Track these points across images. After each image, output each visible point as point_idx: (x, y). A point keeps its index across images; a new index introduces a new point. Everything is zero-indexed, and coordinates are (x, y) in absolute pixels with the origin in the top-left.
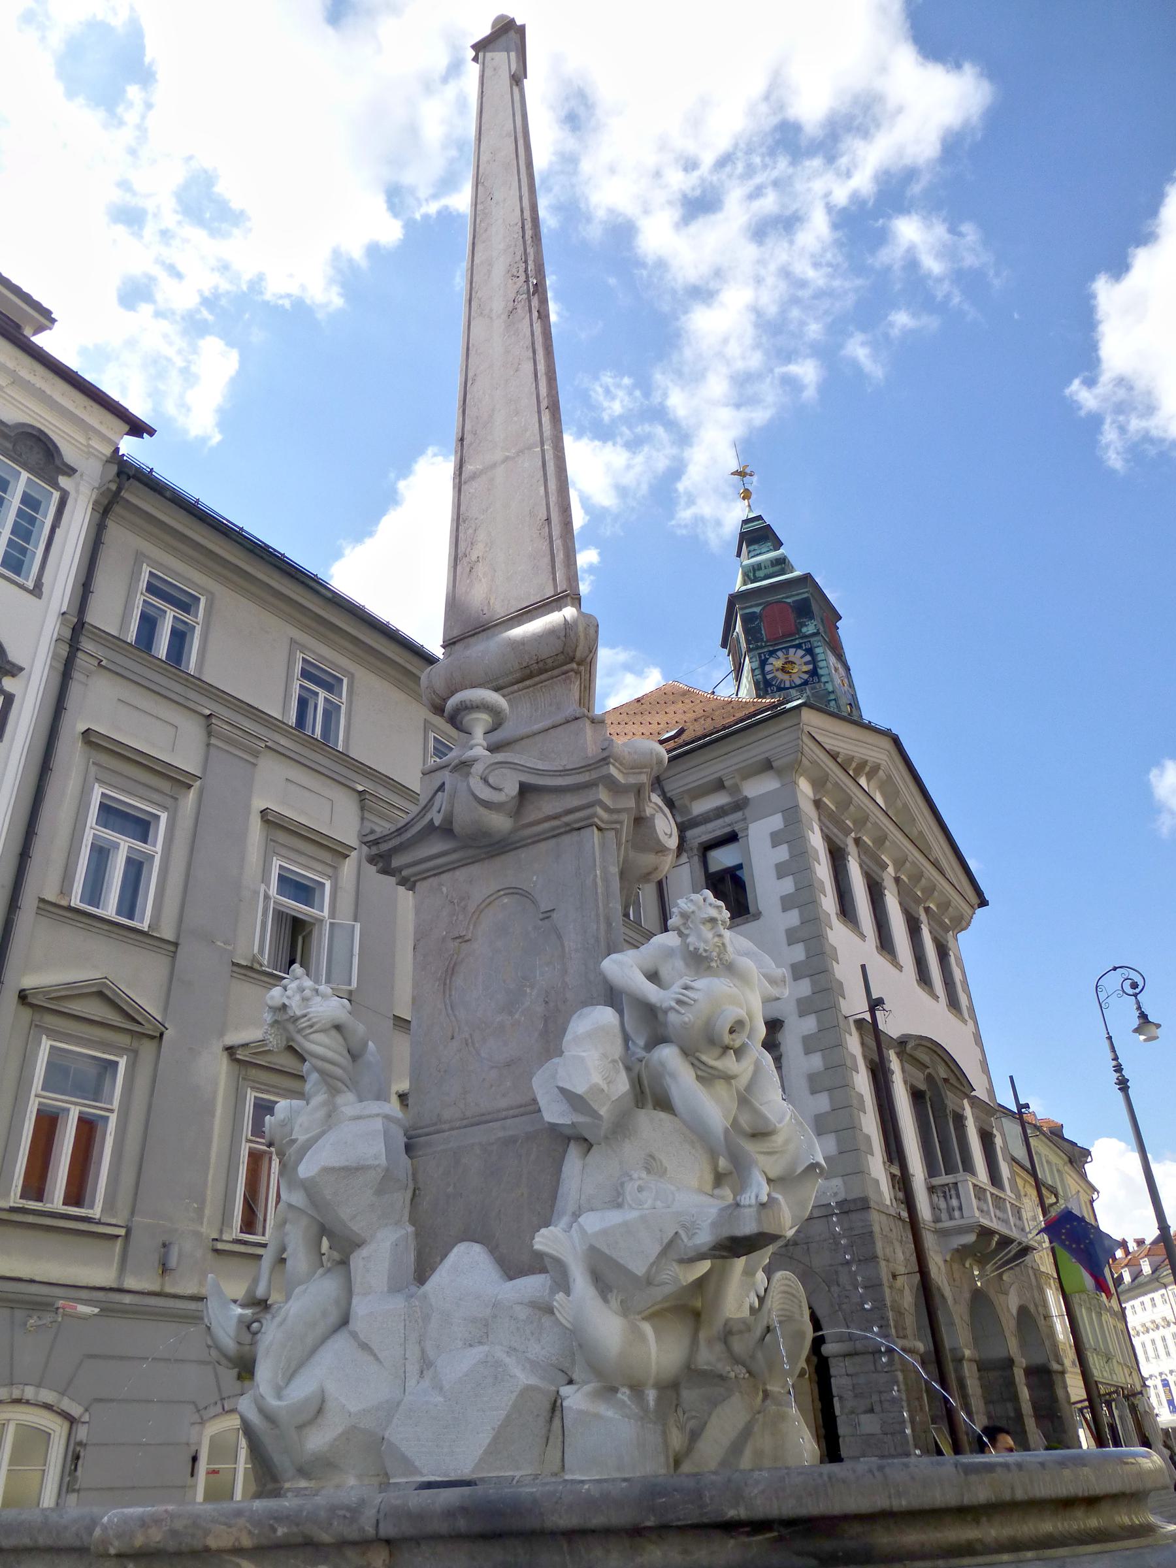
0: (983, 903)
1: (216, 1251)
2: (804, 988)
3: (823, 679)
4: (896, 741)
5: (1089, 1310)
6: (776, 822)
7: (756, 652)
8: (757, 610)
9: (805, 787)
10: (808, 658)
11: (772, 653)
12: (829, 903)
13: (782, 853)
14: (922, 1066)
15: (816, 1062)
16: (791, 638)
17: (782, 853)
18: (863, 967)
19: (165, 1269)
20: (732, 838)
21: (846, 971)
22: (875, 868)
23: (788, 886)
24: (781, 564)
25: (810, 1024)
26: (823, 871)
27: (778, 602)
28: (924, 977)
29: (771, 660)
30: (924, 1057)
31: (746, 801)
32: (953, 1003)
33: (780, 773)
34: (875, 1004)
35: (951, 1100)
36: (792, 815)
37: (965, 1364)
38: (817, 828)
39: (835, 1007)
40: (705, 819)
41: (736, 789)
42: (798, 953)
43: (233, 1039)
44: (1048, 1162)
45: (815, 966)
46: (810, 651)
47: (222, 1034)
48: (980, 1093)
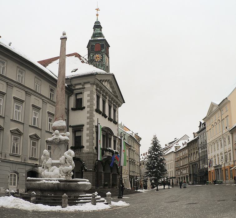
1: (10, 155)
2: (88, 120)
3: (103, 62)
4: (113, 76)
5: (132, 165)
6: (89, 93)
7: (92, 53)
8: (94, 44)
9: (95, 87)
10: (101, 57)
11: (95, 54)
13: (89, 98)
14: (105, 132)
15: (88, 132)
16: (99, 52)
17: (89, 98)
18: (98, 118)
19: (5, 157)
20: (81, 93)
21: (95, 119)
22: (105, 99)
24: (101, 35)
25: (88, 126)
26: (95, 102)
27: (98, 43)
29: (95, 55)
33: (91, 84)
34: (98, 124)
37: (102, 173)
38: (95, 94)
42: (88, 115)
43: (11, 129)
44: (132, 141)
45: (91, 118)
46: (102, 55)
47: (9, 129)
48: (115, 135)
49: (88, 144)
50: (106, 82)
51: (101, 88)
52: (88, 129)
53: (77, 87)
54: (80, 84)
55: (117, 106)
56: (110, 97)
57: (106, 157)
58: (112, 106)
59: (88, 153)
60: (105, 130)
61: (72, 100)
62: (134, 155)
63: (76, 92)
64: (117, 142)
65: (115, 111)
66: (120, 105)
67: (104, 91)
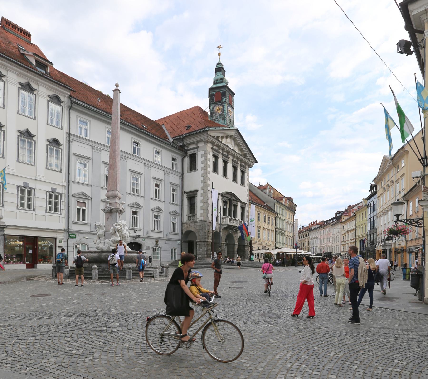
0: (256, 162)
2: (202, 185)
9: (210, 145)
12: (211, 168)
21: (210, 183)
23: (202, 166)
25: (202, 191)
26: (211, 163)
28: (235, 179)
30: (229, 196)
31: (198, 147)
32: (242, 183)
33: (204, 142)
35: (234, 203)
36: (205, 151)
39: (207, 189)
40: (191, 149)
41: (196, 144)
42: (202, 179)
45: (205, 182)
49: (202, 211)
50: (228, 139)
51: (219, 146)
52: (202, 195)
53: (191, 147)
54: (193, 143)
55: (247, 167)
56: (233, 156)
57: (226, 226)
58: (239, 167)
59: (202, 221)
60: (227, 195)
61: (187, 161)
62: (283, 226)
63: (190, 152)
64: (246, 208)
65: (243, 172)
66: (250, 165)
67: (223, 149)
